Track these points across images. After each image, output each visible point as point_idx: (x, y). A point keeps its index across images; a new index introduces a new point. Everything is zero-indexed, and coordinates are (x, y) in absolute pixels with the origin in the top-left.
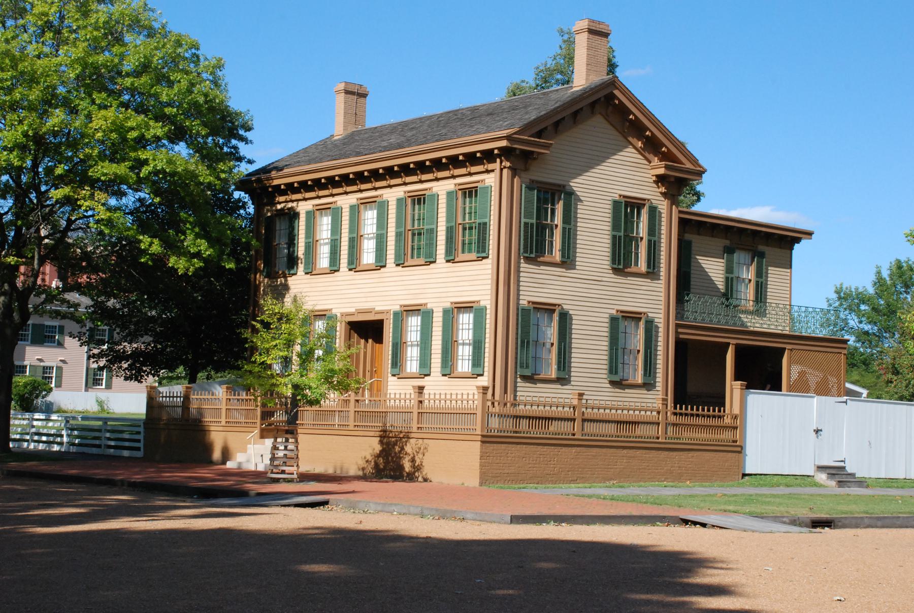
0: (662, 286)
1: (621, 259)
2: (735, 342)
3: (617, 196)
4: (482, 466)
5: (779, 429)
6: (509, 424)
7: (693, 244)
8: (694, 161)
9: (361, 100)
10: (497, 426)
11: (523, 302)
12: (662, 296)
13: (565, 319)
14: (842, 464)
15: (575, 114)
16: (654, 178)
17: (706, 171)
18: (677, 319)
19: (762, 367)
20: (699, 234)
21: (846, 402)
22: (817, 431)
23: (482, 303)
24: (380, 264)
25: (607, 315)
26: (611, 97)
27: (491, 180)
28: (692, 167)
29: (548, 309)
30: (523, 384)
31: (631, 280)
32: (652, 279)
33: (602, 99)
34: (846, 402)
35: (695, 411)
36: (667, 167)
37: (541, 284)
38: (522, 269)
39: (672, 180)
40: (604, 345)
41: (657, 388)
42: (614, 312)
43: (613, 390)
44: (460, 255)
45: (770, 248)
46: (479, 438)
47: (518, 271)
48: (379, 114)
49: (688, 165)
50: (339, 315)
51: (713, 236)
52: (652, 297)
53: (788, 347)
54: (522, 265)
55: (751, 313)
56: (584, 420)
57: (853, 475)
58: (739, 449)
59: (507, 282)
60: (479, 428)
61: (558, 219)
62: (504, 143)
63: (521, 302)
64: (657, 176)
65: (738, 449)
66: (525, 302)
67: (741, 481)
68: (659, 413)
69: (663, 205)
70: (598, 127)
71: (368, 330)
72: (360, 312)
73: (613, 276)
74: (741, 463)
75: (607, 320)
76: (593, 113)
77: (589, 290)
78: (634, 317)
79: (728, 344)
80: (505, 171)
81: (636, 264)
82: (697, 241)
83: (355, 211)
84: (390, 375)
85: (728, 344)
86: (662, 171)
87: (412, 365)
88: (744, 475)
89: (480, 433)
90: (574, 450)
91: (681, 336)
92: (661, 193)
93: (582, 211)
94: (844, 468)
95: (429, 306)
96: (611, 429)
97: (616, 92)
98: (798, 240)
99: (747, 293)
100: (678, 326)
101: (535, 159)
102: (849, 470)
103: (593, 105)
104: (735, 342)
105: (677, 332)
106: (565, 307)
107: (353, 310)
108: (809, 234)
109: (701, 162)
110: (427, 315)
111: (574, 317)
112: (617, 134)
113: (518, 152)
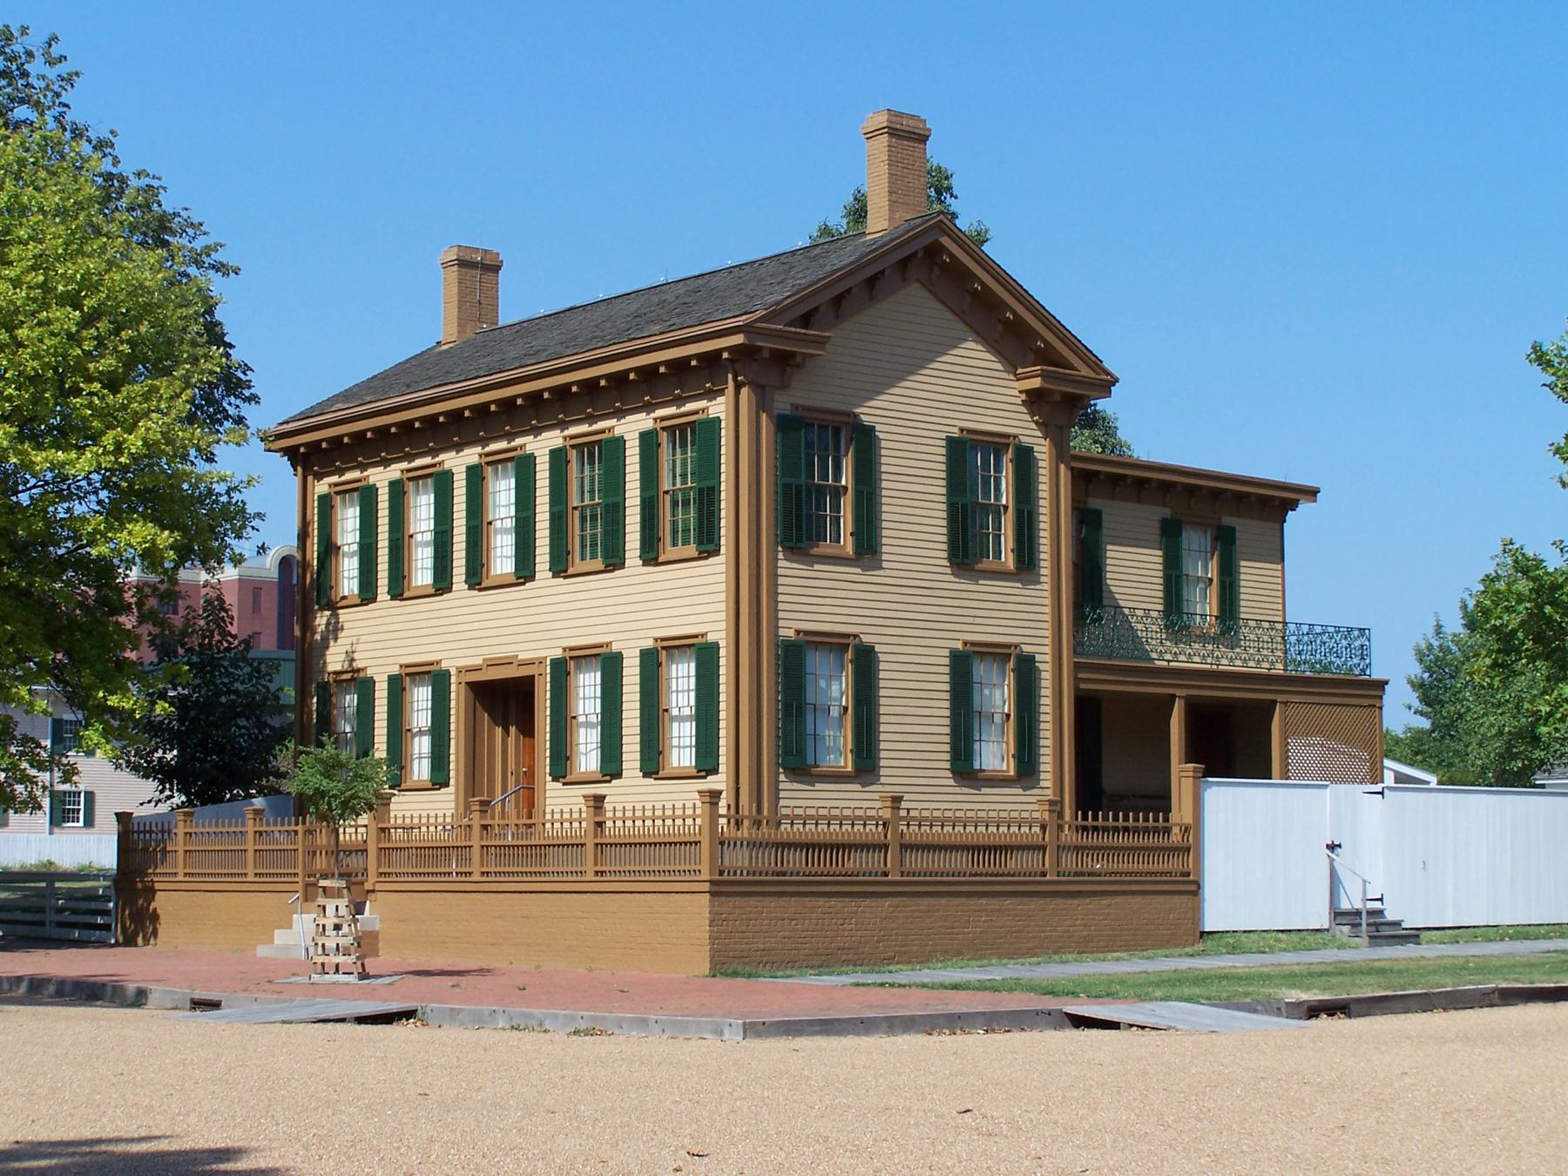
0: (1046, 594)
1: (965, 549)
3: (956, 430)
4: (713, 938)
5: (1261, 847)
6: (767, 860)
7: (1104, 517)
8: (1094, 363)
9: (490, 276)
10: (747, 863)
11: (787, 632)
13: (865, 663)
14: (1377, 905)
15: (872, 282)
16: (1024, 396)
17: (1117, 380)
19: (1234, 737)
20: (1113, 498)
21: (1382, 793)
22: (1332, 847)
23: (711, 638)
24: (525, 571)
26: (934, 252)
27: (718, 408)
28: (1092, 375)
29: (836, 644)
31: (986, 585)
32: (1026, 583)
33: (920, 254)
36: (1044, 375)
37: (816, 598)
38: (780, 571)
39: (1057, 398)
40: (941, 708)
41: (1043, 784)
42: (959, 645)
43: (958, 790)
44: (669, 548)
46: (706, 887)
47: (774, 576)
48: (518, 301)
49: (1085, 371)
50: (453, 671)
51: (1139, 501)
52: (1026, 615)
53: (1280, 698)
54: (780, 563)
55: (1215, 640)
56: (905, 847)
57: (1397, 924)
58: (1194, 888)
59: (754, 599)
60: (705, 867)
61: (846, 479)
62: (739, 339)
63: (782, 632)
64: (1028, 392)
65: (1191, 887)
66: (791, 633)
67: (1200, 947)
68: (1043, 828)
69: (1043, 450)
70: (915, 304)
71: (505, 699)
72: (492, 664)
73: (952, 578)
74: (1197, 913)
76: (904, 279)
77: (907, 603)
78: (998, 653)
79: (1174, 697)
80: (745, 391)
81: (998, 555)
82: (1113, 512)
83: (475, 476)
84: (549, 778)
85: (1174, 697)
86: (1036, 383)
87: (588, 758)
88: (1203, 933)
89: (705, 876)
90: (887, 902)
91: (1083, 686)
92: (1036, 423)
93: (889, 463)
95: (615, 647)
96: (960, 862)
97: (945, 241)
98: (1293, 505)
99: (1204, 606)
100: (1078, 667)
101: (798, 366)
102: (1390, 916)
103: (905, 262)
106: (865, 639)
107: (478, 661)
108: (1312, 493)
109: (1106, 364)
110: (611, 664)
112: (952, 317)
113: (766, 354)
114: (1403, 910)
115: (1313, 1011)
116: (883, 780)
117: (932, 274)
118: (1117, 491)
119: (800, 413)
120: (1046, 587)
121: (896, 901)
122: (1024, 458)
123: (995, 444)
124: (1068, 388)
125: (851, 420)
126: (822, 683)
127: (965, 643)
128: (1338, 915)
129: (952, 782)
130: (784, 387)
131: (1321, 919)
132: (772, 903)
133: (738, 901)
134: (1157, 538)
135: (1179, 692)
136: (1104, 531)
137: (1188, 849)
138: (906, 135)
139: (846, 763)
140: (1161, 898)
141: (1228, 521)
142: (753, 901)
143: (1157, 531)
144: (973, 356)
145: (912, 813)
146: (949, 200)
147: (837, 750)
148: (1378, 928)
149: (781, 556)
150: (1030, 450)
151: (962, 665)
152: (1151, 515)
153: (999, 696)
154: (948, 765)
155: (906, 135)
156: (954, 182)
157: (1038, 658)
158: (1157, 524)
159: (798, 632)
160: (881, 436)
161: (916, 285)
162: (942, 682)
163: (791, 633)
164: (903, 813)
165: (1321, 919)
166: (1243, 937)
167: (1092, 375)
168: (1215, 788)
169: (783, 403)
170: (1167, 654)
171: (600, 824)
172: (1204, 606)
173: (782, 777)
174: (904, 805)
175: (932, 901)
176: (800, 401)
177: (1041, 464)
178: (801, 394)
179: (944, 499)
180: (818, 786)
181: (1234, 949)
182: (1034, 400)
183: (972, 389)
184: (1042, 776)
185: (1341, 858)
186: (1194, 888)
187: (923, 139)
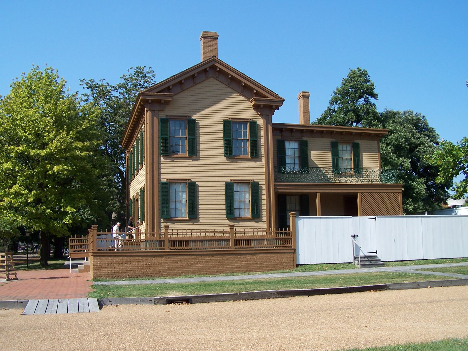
0: (264, 164)
1: (230, 152)
2: (320, 191)
7: (309, 142)
8: (275, 95)
10: (145, 247)
11: (164, 179)
12: (264, 170)
14: (375, 254)
18: (275, 181)
21: (375, 219)
22: (354, 236)
25: (224, 183)
26: (214, 68)
28: (275, 99)
31: (240, 163)
34: (375, 219)
35: (284, 231)
36: (255, 100)
40: (223, 199)
41: (263, 220)
42: (229, 181)
45: (361, 141)
47: (159, 164)
49: (272, 98)
51: (322, 137)
53: (359, 191)
55: (351, 176)
57: (379, 260)
58: (293, 251)
65: (294, 251)
66: (165, 180)
69: (261, 122)
70: (213, 85)
73: (227, 161)
75: (224, 186)
76: (207, 78)
82: (311, 141)
86: (253, 103)
88: (298, 265)
94: (376, 257)
97: (217, 65)
99: (348, 165)
104: (320, 191)
105: (275, 189)
106: (193, 180)
109: (280, 95)
111: (200, 185)
115: (170, 301)
116: (200, 221)
117: (212, 74)
118: (283, 132)
119: (168, 117)
120: (264, 162)
121: (167, 257)
122: (254, 126)
123: (243, 122)
124: (267, 103)
125: (187, 118)
126: (180, 194)
128: (355, 258)
130: (162, 110)
131: (350, 259)
132: (118, 258)
133: (104, 258)
134: (330, 148)
135: (317, 191)
136: (309, 147)
137: (291, 239)
139: (185, 215)
140: (279, 255)
141: (356, 141)
142: (110, 258)
144: (237, 97)
145: (174, 231)
146: (368, 78)
147: (183, 213)
148: (370, 261)
149: (162, 158)
150: (256, 123)
151: (229, 187)
152: (327, 141)
153: (246, 195)
154: (225, 216)
155: (210, 38)
156: (368, 72)
157: (259, 183)
158: (330, 144)
159: (167, 179)
160: (199, 122)
161: (212, 78)
162: (223, 191)
163: (165, 180)
164: (234, 230)
165: (350, 259)
166: (314, 267)
167: (275, 99)
169: (163, 115)
170: (338, 181)
172: (348, 165)
173: (162, 221)
174: (235, 228)
175: (182, 257)
176: (168, 114)
177: (261, 126)
179: (223, 139)
181: (306, 270)
182: (256, 107)
183: (240, 107)
184: (263, 218)
185: (359, 241)
186: (293, 251)
187: (216, 38)
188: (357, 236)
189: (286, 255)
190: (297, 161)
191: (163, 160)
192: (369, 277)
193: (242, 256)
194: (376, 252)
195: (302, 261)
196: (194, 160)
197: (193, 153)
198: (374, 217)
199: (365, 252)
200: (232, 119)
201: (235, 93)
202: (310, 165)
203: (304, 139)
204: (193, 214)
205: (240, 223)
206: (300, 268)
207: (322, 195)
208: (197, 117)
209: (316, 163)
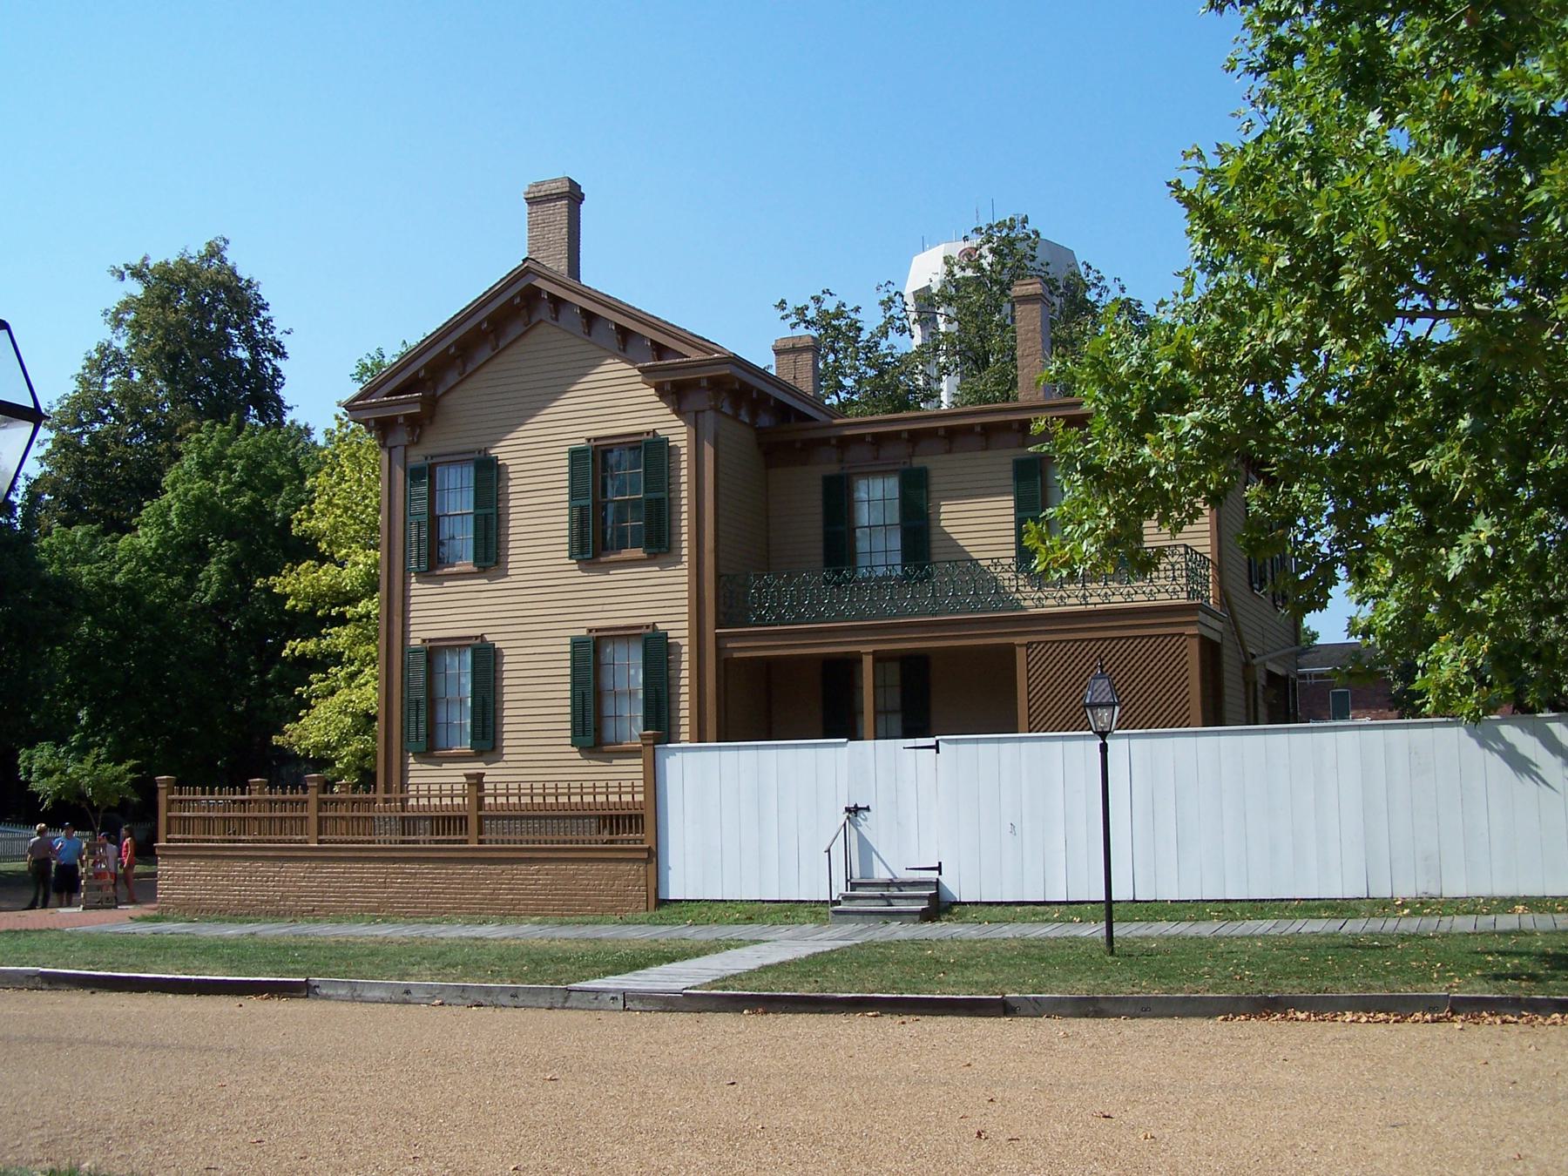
2: (870, 648)
11: (415, 642)
13: (486, 659)
14: (934, 875)
22: (854, 811)
25: (568, 641)
29: (455, 645)
30: (418, 766)
34: (937, 747)
43: (585, 763)
49: (696, 356)
53: (1017, 640)
65: (652, 857)
66: (419, 642)
82: (939, 466)
93: (516, 486)
104: (870, 648)
105: (718, 649)
114: (959, 886)
127: (590, 631)
129: (578, 756)
138: (565, 201)
143: (1011, 474)
144: (615, 370)
153: (628, 671)
154: (569, 741)
157: (670, 634)
158: (1010, 467)
163: (419, 642)
168: (679, 755)
169: (417, 457)
171: (481, 800)
173: (411, 760)
178: (436, 443)
180: (445, 766)
185: (869, 826)
188: (868, 809)
189: (623, 867)
190: (896, 542)
191: (415, 586)
192: (912, 960)
193: (499, 868)
194: (939, 869)
195: (676, 888)
196: (491, 579)
197: (490, 556)
198: (931, 741)
199: (893, 863)
200: (596, 439)
201: (606, 358)
202: (938, 553)
203: (917, 462)
204: (487, 740)
205: (615, 762)
206: (663, 911)
207: (879, 658)
208: (502, 452)
209: (961, 543)
